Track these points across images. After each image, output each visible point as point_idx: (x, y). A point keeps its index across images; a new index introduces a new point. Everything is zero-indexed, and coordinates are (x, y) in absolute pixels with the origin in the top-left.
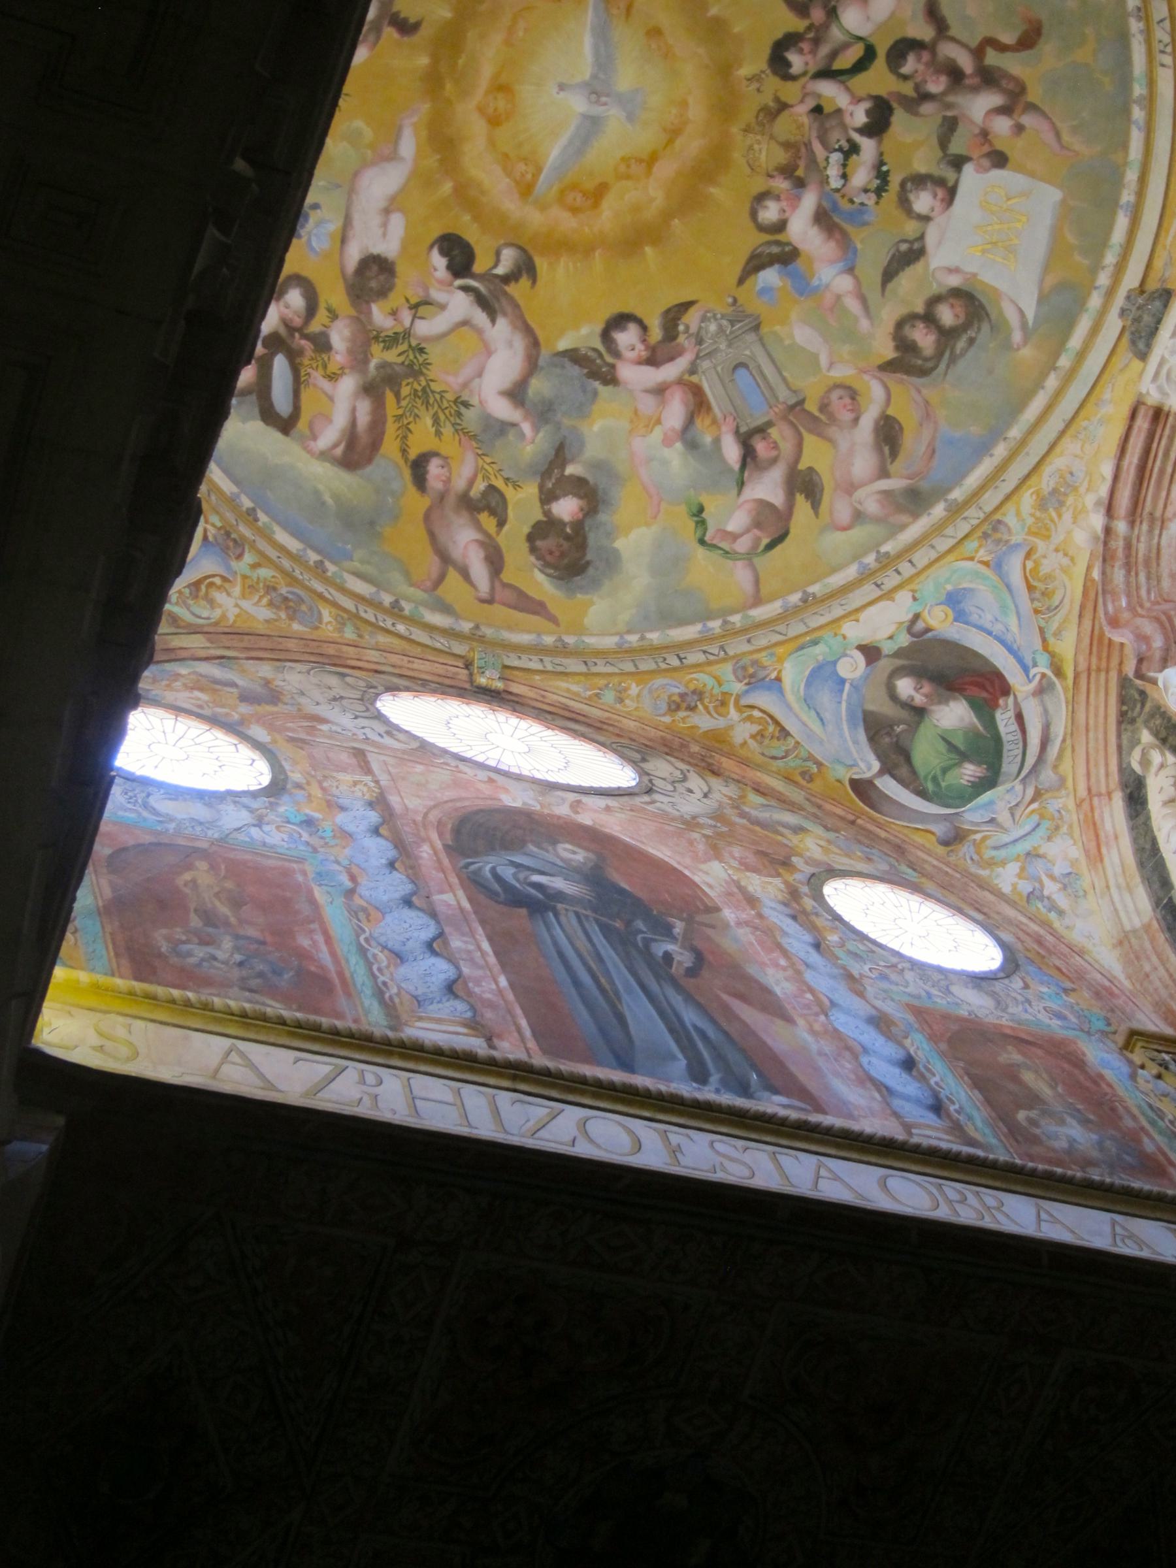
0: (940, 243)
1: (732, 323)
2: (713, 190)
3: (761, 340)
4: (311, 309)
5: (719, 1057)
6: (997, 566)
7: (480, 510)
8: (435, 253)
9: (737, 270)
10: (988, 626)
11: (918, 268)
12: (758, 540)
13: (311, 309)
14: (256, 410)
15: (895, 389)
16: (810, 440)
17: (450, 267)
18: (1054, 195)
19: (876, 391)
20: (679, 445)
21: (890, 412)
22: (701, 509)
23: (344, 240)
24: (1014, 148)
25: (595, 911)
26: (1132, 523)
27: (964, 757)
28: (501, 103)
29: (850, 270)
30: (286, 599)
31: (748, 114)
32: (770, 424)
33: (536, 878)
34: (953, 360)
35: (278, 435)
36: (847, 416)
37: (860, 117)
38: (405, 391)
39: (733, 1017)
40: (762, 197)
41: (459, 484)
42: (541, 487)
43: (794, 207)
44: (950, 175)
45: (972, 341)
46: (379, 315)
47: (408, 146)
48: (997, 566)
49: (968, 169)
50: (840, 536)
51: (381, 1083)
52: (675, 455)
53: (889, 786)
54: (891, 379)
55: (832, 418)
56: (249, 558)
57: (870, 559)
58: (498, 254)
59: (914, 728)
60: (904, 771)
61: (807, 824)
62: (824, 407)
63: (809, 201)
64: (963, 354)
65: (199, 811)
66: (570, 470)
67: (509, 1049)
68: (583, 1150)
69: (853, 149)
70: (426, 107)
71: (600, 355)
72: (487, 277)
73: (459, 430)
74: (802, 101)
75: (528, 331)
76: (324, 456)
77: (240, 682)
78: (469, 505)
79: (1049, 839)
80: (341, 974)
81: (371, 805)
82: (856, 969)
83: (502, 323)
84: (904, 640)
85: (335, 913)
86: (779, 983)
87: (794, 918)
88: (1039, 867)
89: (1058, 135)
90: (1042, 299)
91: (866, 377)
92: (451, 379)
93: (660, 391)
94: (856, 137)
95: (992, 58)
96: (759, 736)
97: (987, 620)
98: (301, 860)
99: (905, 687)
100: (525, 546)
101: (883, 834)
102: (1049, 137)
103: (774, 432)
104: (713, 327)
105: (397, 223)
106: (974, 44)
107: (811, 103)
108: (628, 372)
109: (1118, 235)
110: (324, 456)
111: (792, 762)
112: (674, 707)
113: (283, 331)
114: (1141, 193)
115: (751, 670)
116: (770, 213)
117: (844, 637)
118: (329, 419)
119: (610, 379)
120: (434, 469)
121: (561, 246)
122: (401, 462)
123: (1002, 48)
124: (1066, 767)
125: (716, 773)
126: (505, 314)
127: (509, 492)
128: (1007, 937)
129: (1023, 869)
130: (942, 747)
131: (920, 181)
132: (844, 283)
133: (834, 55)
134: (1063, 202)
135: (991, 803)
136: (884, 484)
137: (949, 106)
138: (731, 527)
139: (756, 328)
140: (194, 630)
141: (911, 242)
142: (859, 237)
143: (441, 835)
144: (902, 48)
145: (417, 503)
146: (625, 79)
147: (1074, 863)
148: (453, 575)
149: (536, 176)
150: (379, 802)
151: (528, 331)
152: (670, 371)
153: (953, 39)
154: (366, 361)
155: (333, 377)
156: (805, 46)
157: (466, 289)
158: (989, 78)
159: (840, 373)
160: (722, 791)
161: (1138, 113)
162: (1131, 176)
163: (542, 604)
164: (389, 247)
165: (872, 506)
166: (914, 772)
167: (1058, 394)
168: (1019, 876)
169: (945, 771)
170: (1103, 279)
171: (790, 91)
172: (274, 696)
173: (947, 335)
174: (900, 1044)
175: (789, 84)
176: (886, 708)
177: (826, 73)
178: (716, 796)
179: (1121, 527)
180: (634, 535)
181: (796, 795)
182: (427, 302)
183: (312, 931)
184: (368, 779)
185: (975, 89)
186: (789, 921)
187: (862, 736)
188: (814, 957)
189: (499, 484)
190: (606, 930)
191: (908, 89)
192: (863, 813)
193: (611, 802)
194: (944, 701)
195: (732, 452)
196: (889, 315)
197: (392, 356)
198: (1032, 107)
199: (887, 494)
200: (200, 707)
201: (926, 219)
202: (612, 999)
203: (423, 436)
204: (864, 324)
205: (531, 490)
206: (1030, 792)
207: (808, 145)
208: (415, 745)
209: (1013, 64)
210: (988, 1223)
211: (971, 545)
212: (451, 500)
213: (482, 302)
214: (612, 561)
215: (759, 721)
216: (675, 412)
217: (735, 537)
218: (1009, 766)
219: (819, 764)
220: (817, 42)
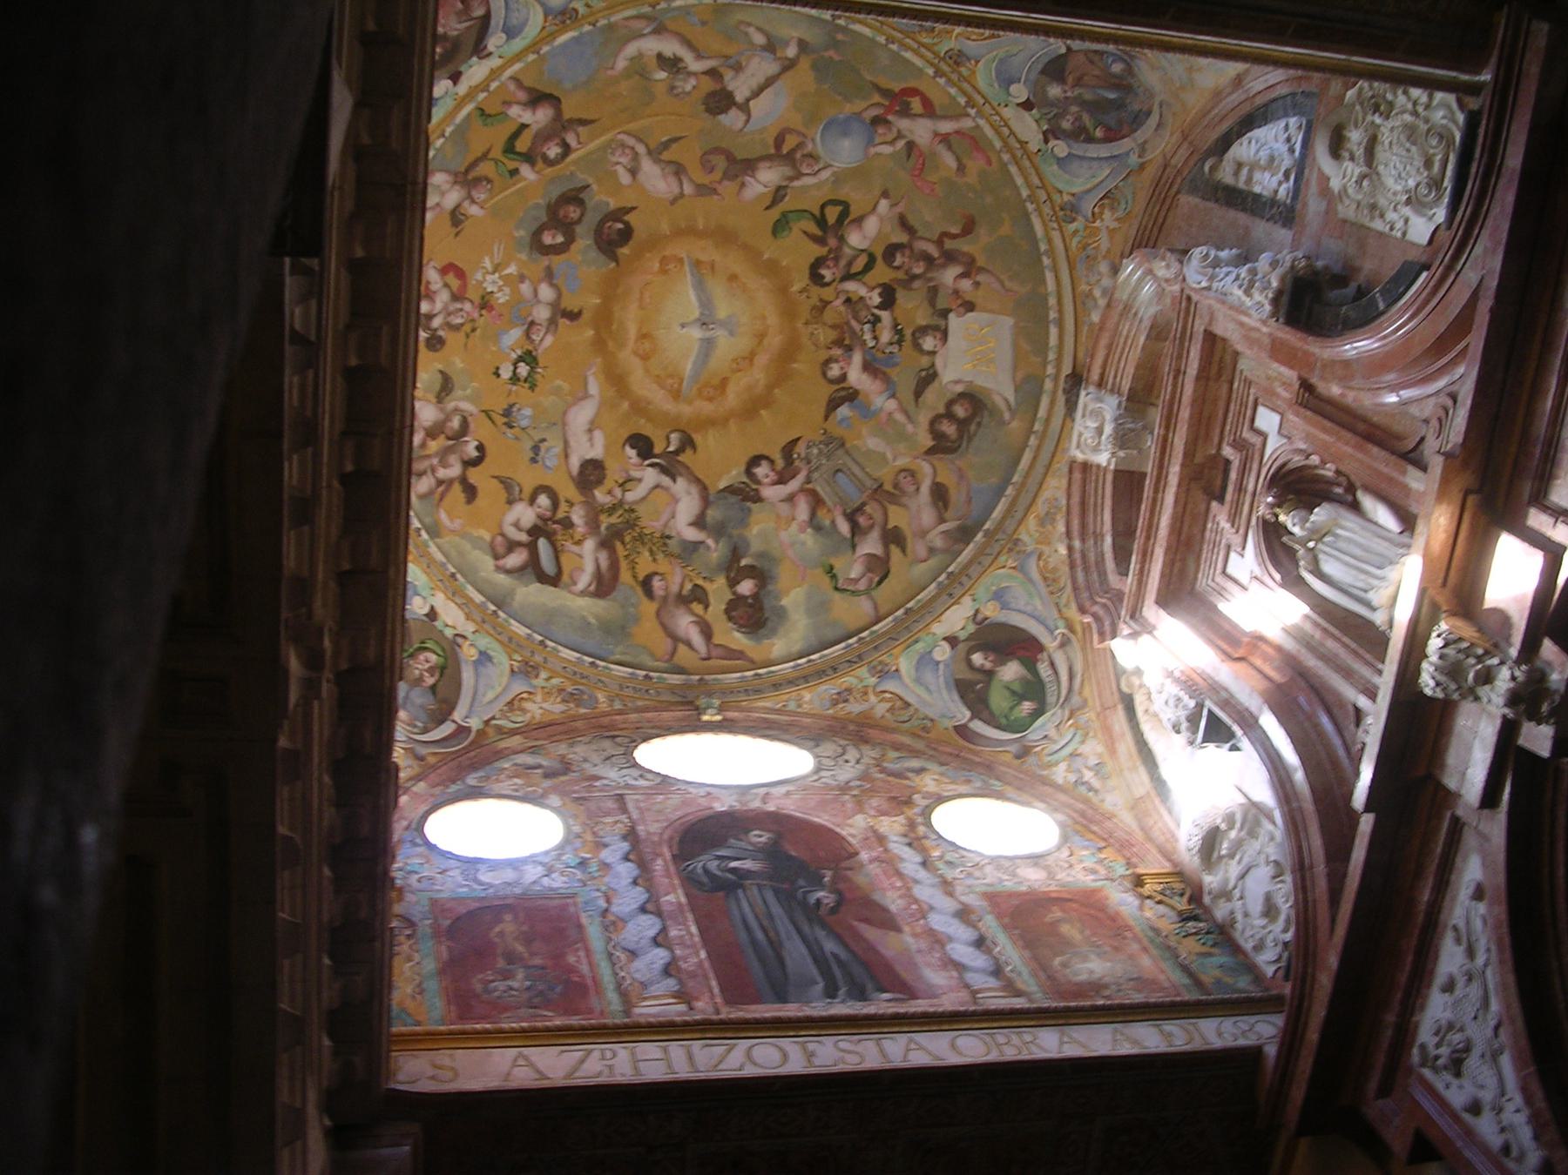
0: (945, 366)
1: (827, 445)
2: (795, 365)
3: (847, 452)
4: (555, 505)
5: (849, 976)
6: (1021, 568)
7: (692, 602)
8: (628, 448)
9: (822, 411)
10: (1023, 608)
11: (935, 384)
12: (871, 580)
13: (555, 505)
14: (533, 577)
15: (936, 463)
16: (892, 509)
17: (639, 455)
18: (1009, 321)
19: (925, 468)
20: (809, 530)
21: (938, 480)
22: (832, 568)
23: (567, 456)
24: (978, 297)
25: (771, 878)
26: (1083, 541)
27: (1021, 697)
28: (647, 345)
29: (893, 396)
30: (572, 694)
31: (805, 313)
32: (864, 504)
33: (734, 864)
34: (970, 440)
35: (553, 589)
36: (912, 488)
37: (877, 300)
38: (628, 539)
39: (859, 937)
40: (827, 363)
41: (675, 588)
42: (728, 578)
43: (849, 364)
44: (942, 323)
45: (979, 424)
46: (600, 495)
47: (593, 388)
48: (1021, 568)
49: (952, 316)
51: (615, 1055)
52: (809, 538)
53: (978, 726)
54: (935, 459)
55: (903, 493)
56: (543, 675)
58: (668, 438)
59: (988, 684)
60: (985, 714)
61: (929, 765)
62: (896, 486)
63: (857, 358)
64: (975, 435)
65: (509, 875)
66: (743, 562)
67: (704, 1008)
68: (750, 1071)
69: (877, 319)
70: (599, 360)
71: (748, 486)
73: (669, 555)
74: (837, 298)
75: (698, 481)
76: (583, 593)
77: (545, 763)
78: (684, 600)
79: (1083, 742)
80: (594, 978)
81: (625, 838)
82: (950, 874)
83: (680, 480)
84: (972, 628)
85: (594, 932)
86: (893, 901)
87: (910, 845)
88: (1078, 762)
89: (1003, 286)
91: (918, 461)
92: (655, 524)
93: (790, 499)
94: (876, 311)
95: (949, 244)
96: (891, 710)
97: (1021, 604)
98: (574, 895)
99: (977, 658)
100: (724, 617)
101: (977, 759)
102: (996, 285)
103: (868, 509)
104: (815, 451)
105: (598, 436)
106: (935, 238)
107: (842, 298)
109: (1053, 340)
110: (583, 593)
111: (915, 722)
112: (835, 703)
113: (540, 523)
114: (1060, 311)
115: (879, 668)
116: (835, 371)
117: (934, 634)
118: (583, 570)
119: (758, 499)
120: (657, 583)
122: (634, 584)
123: (954, 237)
124: (1087, 692)
125: (866, 742)
126: (681, 475)
129: (1069, 766)
130: (1007, 693)
131: (923, 330)
132: (891, 405)
133: (850, 264)
135: (1043, 725)
136: (943, 527)
137: (930, 280)
138: (853, 576)
139: (843, 445)
140: (513, 732)
141: (927, 369)
142: (893, 373)
143: (670, 847)
144: (891, 251)
145: (649, 608)
146: (722, 312)
147: (1100, 755)
148: (682, 648)
149: (681, 384)
150: (631, 835)
151: (698, 481)
152: (794, 485)
153: (922, 238)
154: (598, 527)
155: (579, 543)
156: (830, 263)
158: (950, 257)
159: (902, 462)
160: (870, 753)
161: (1046, 261)
162: (1052, 301)
163: (741, 652)
164: (596, 452)
165: (939, 543)
166: (992, 714)
167: (1039, 448)
169: (1012, 708)
170: (1050, 370)
171: (827, 293)
172: (566, 767)
173: (963, 424)
174: (974, 927)
175: (826, 289)
176: (968, 675)
177: (848, 277)
178: (865, 760)
179: (1077, 544)
181: (920, 745)
182: (629, 480)
183: (577, 950)
184: (623, 818)
185: (944, 266)
186: (907, 849)
187: (956, 697)
188: (922, 874)
189: (700, 582)
190: (776, 892)
191: (901, 275)
192: (965, 748)
194: (1003, 663)
195: (844, 527)
196: (924, 418)
197: (614, 519)
201: (933, 353)
202: (776, 945)
203: (645, 565)
204: (910, 428)
205: (721, 581)
206: (1067, 713)
207: (847, 323)
208: (658, 780)
209: (964, 246)
210: (1025, 1056)
211: (1002, 558)
212: (671, 599)
213: (664, 470)
214: (781, 614)
215: (889, 700)
216: (803, 510)
217: (856, 581)
218: (1051, 699)
219: (932, 720)
220: (836, 259)
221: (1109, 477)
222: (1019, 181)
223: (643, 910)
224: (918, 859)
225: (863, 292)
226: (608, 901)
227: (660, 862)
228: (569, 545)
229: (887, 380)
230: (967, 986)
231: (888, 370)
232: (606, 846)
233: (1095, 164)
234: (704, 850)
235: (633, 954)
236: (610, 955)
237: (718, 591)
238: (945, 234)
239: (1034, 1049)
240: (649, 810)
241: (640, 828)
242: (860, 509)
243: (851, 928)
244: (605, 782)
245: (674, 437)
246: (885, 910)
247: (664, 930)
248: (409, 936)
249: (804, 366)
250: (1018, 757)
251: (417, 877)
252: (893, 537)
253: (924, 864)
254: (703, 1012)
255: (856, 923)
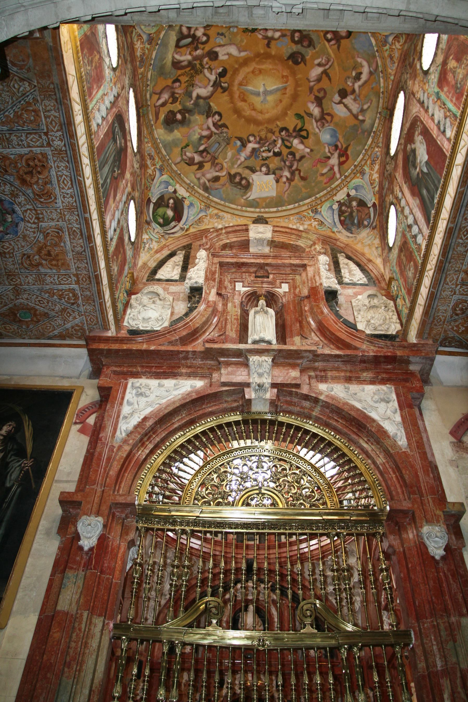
6: (201, 210)
11: (251, 173)
22: (188, 146)
24: (281, 184)
27: (163, 218)
29: (245, 159)
34: (235, 187)
38: (192, 71)
40: (253, 135)
41: (176, 91)
42: (181, 110)
44: (271, 173)
45: (240, 189)
46: (206, 60)
48: (201, 210)
49: (273, 176)
50: (193, 177)
52: (197, 136)
53: (152, 206)
55: (215, 166)
57: (192, 185)
58: (226, 83)
62: (217, 164)
63: (256, 146)
69: (270, 151)
72: (220, 82)
76: (173, 57)
78: (173, 95)
84: (180, 197)
90: (253, 200)
93: (209, 128)
95: (297, 172)
97: (190, 212)
99: (171, 201)
100: (168, 110)
102: (285, 189)
103: (209, 155)
106: (299, 168)
107: (276, 139)
108: (210, 120)
109: (272, 210)
110: (173, 57)
112: (149, 155)
116: (251, 139)
119: (208, 117)
120: (178, 84)
121: (231, 96)
123: (299, 174)
127: (178, 103)
131: (268, 167)
132: (243, 159)
134: (274, 197)
142: (253, 159)
145: (169, 82)
152: (213, 129)
155: (190, 54)
157: (216, 78)
158: (293, 173)
159: (225, 165)
165: (202, 181)
169: (159, 216)
176: (166, 199)
179: (224, 231)
180: (178, 134)
185: (289, 171)
189: (179, 100)
191: (285, 158)
195: (202, 148)
196: (240, 170)
197: (198, 66)
198: (290, 184)
199: (205, 183)
201: (261, 171)
204: (236, 166)
205: (180, 107)
207: (267, 142)
209: (297, 177)
212: (173, 90)
213: (215, 82)
214: (171, 131)
216: (205, 133)
217: (185, 155)
218: (165, 228)
221: (246, 238)
222: (322, 194)
225: (279, 145)
228: (189, 50)
229: (249, 157)
231: (253, 156)
233: (332, 218)
237: (177, 107)
238: (300, 171)
242: (208, 153)
245: (226, 85)
249: (252, 127)
250: (146, 221)
252: (201, 165)
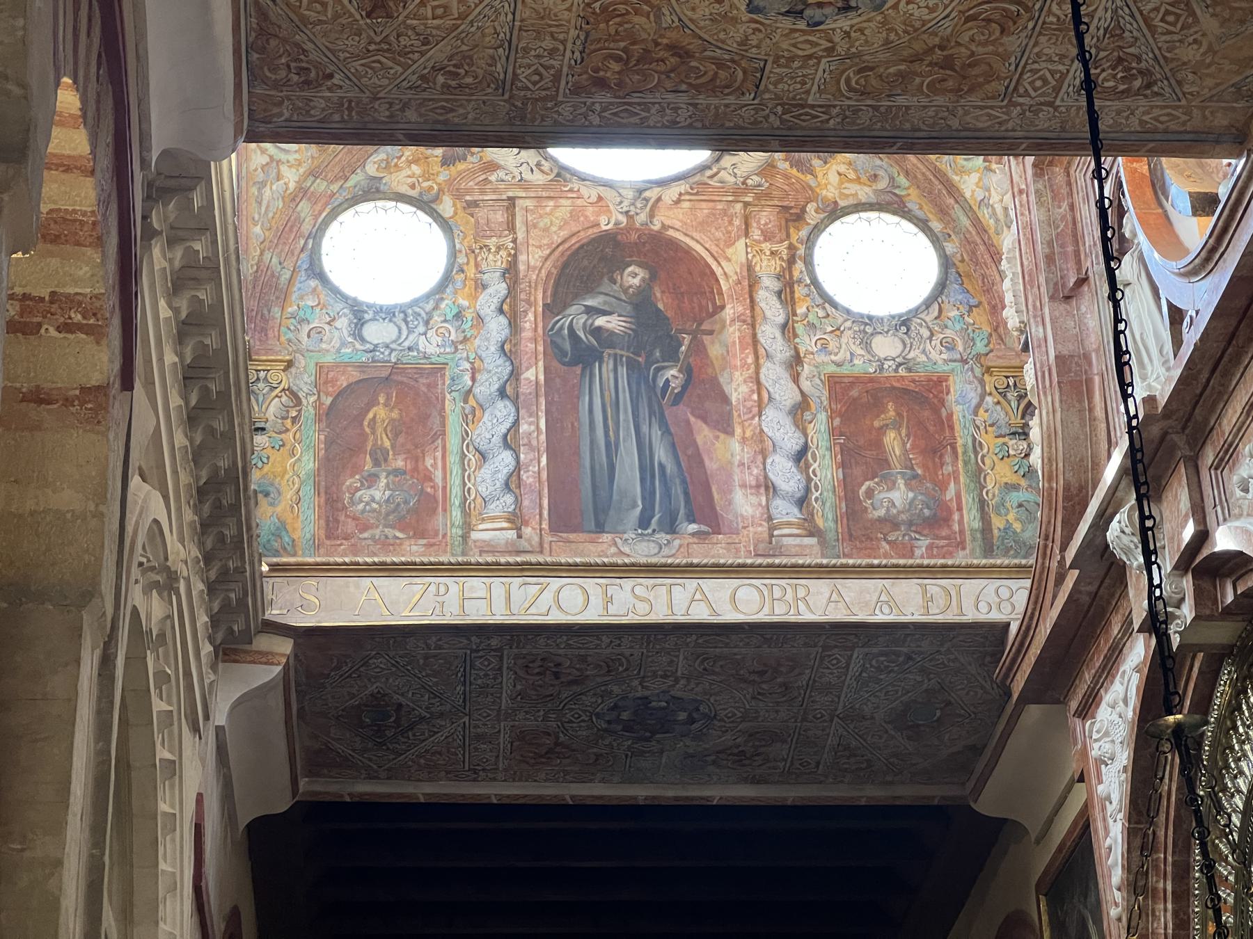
33: (601, 321)
80: (444, 488)
86: (737, 389)
87: (779, 294)
128: (950, 248)
129: (980, 179)
150: (511, 272)
168: (977, 185)
186: (774, 301)
190: (632, 365)
193: (682, 187)
200: (413, 187)
223: (502, 393)
224: (781, 319)
226: (473, 379)
227: (531, 316)
230: (770, 518)
232: (484, 287)
234: (577, 296)
235: (483, 456)
236: (463, 456)
239: (801, 605)
240: (535, 226)
241: (522, 258)
243: (688, 422)
244: (501, 174)
246: (725, 399)
247: (516, 423)
248: (294, 419)
251: (306, 329)
253: (784, 327)
254: (529, 541)
255: (692, 419)
